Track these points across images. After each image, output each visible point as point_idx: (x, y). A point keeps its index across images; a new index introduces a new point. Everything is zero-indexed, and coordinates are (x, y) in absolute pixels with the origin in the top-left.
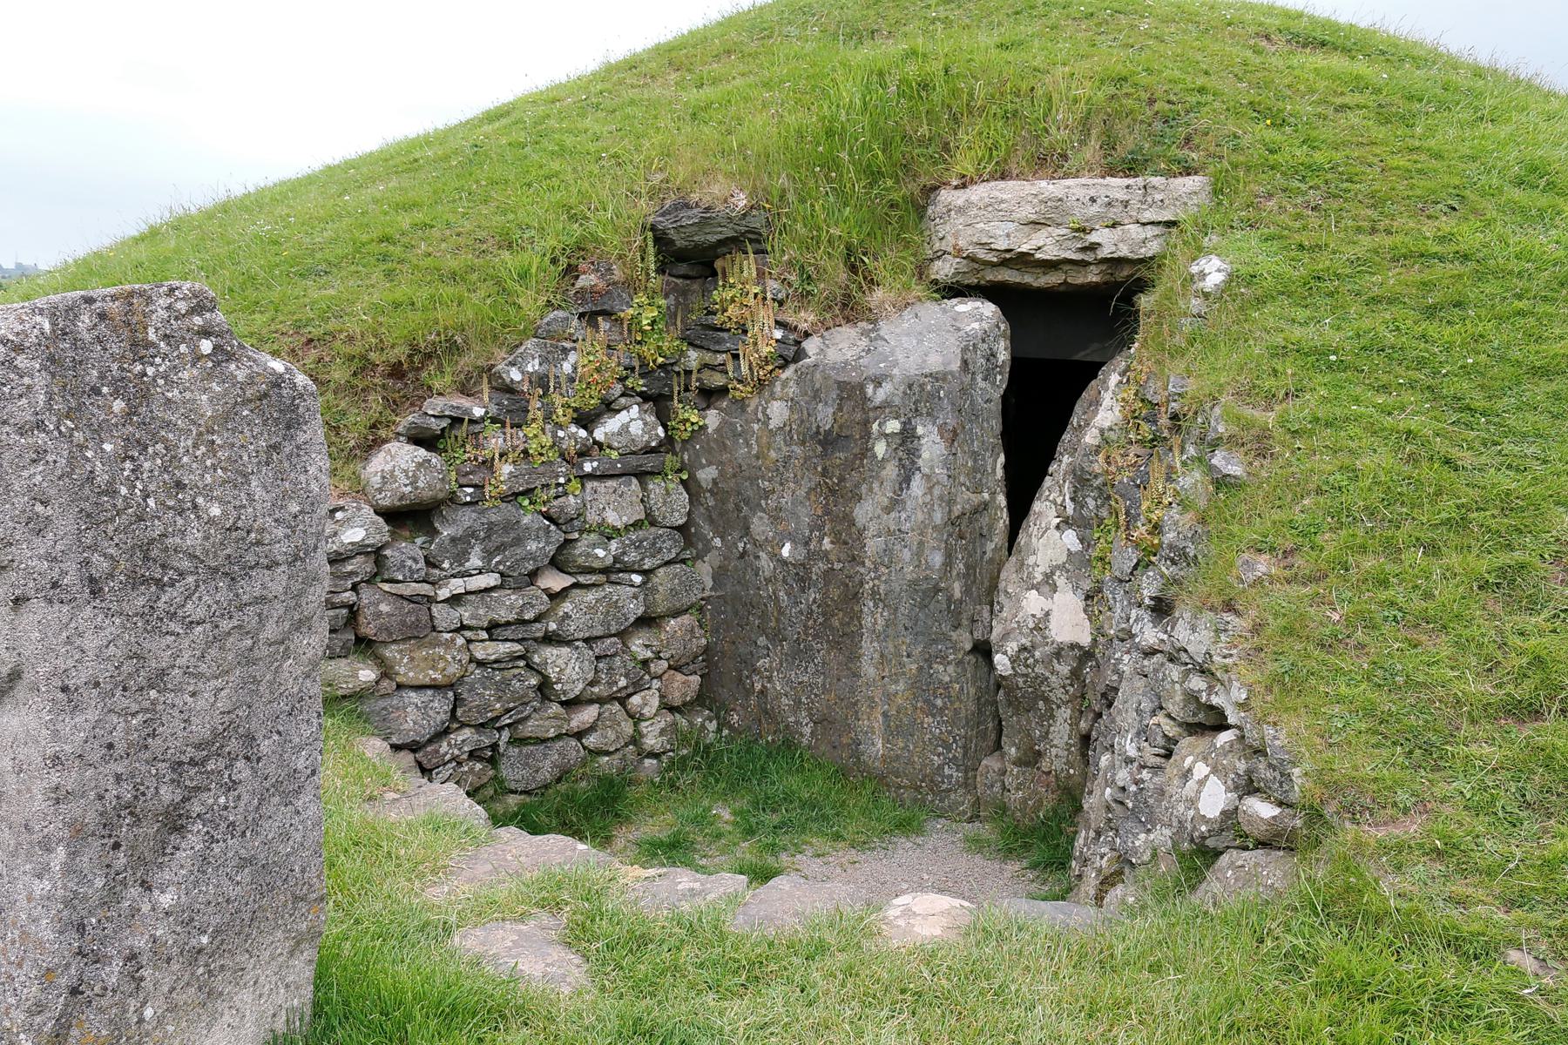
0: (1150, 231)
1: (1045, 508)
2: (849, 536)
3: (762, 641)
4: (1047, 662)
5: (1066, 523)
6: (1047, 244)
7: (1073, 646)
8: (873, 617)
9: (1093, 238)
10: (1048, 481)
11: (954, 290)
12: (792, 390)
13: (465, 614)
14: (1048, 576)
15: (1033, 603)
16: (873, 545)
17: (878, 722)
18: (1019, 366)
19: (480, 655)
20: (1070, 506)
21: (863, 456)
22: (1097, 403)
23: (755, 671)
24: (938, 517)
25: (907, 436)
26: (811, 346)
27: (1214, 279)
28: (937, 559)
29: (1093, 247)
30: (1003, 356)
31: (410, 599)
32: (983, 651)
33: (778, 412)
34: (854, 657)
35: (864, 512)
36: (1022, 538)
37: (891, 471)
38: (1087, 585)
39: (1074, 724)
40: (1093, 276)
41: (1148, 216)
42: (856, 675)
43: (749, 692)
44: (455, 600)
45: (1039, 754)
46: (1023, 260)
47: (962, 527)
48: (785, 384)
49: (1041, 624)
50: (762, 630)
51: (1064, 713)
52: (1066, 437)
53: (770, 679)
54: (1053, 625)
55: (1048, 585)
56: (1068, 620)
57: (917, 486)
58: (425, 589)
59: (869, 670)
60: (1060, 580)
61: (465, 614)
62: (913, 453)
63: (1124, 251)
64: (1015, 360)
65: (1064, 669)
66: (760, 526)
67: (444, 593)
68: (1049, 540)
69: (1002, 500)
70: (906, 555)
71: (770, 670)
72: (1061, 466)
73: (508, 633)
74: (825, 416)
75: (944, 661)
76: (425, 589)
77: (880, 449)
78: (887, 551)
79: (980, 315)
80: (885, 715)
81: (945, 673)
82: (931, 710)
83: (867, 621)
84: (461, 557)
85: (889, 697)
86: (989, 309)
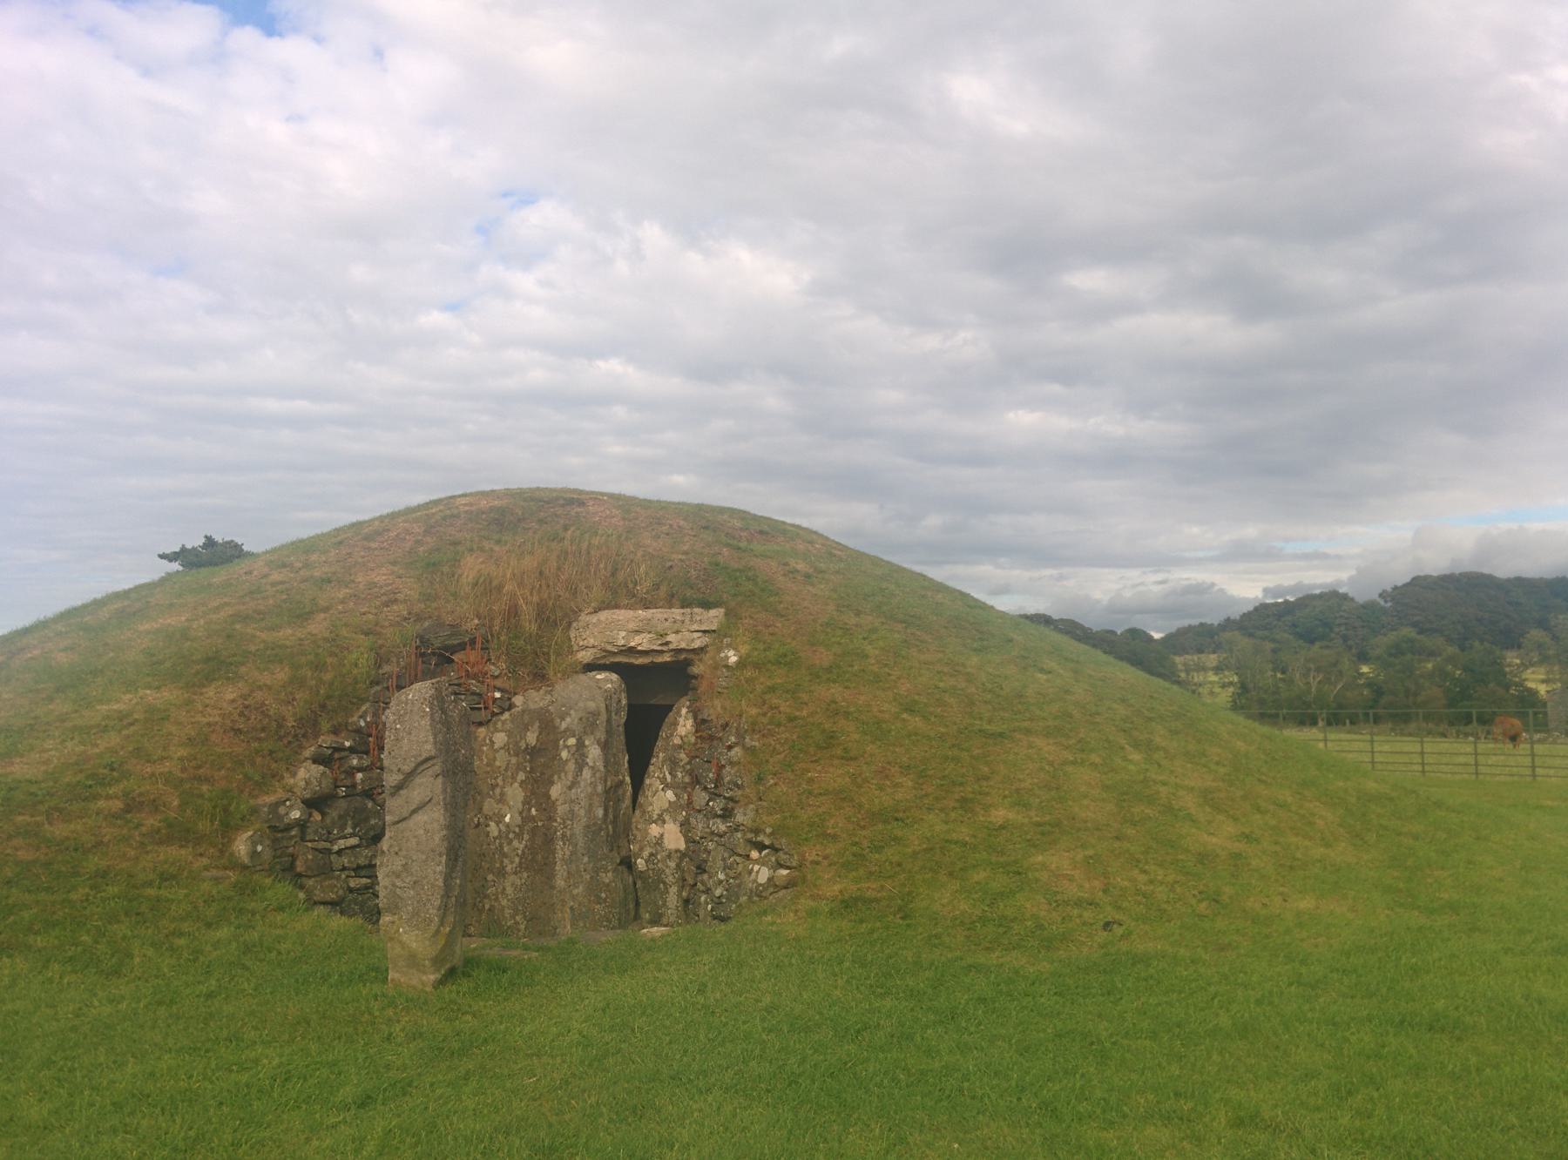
0: (696, 635)
1: (652, 781)
2: (547, 807)
3: (490, 877)
4: (663, 861)
5: (667, 786)
6: (642, 642)
7: (677, 851)
8: (562, 850)
9: (669, 638)
10: (651, 768)
11: (590, 667)
12: (509, 726)
13: (345, 861)
14: (660, 816)
15: (654, 830)
16: (561, 809)
17: (568, 915)
18: (631, 708)
19: (352, 884)
20: (669, 777)
21: (554, 759)
22: (675, 724)
23: (486, 896)
24: (600, 788)
25: (580, 745)
26: (518, 700)
27: (733, 660)
28: (600, 812)
29: (667, 643)
30: (624, 702)
31: (320, 851)
32: (627, 863)
33: (500, 738)
34: (551, 876)
35: (555, 791)
36: (641, 799)
37: (571, 766)
38: (681, 818)
39: (680, 895)
40: (667, 658)
41: (695, 627)
42: (553, 887)
43: (481, 911)
44: (340, 852)
45: (661, 915)
46: (632, 651)
47: (611, 795)
48: (504, 723)
49: (659, 841)
50: (490, 870)
51: (674, 890)
52: (659, 743)
53: (497, 899)
54: (666, 841)
55: (661, 820)
56: (673, 838)
57: (587, 773)
58: (327, 845)
59: (560, 883)
60: (667, 818)
61: (345, 861)
62: (584, 756)
63: (683, 645)
64: (630, 706)
65: (672, 864)
66: (489, 806)
67: (336, 848)
68: (660, 796)
69: (628, 779)
70: (582, 812)
71: (496, 894)
72: (659, 757)
73: (363, 873)
74: (532, 738)
75: (606, 871)
76: (327, 845)
77: (564, 754)
78: (572, 811)
79: (608, 680)
80: (572, 908)
81: (607, 877)
82: (599, 901)
83: (559, 855)
84: (342, 828)
85: (573, 898)
86: (614, 677)
